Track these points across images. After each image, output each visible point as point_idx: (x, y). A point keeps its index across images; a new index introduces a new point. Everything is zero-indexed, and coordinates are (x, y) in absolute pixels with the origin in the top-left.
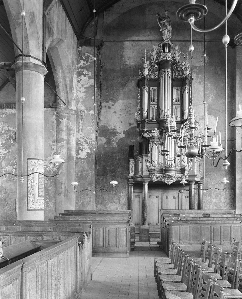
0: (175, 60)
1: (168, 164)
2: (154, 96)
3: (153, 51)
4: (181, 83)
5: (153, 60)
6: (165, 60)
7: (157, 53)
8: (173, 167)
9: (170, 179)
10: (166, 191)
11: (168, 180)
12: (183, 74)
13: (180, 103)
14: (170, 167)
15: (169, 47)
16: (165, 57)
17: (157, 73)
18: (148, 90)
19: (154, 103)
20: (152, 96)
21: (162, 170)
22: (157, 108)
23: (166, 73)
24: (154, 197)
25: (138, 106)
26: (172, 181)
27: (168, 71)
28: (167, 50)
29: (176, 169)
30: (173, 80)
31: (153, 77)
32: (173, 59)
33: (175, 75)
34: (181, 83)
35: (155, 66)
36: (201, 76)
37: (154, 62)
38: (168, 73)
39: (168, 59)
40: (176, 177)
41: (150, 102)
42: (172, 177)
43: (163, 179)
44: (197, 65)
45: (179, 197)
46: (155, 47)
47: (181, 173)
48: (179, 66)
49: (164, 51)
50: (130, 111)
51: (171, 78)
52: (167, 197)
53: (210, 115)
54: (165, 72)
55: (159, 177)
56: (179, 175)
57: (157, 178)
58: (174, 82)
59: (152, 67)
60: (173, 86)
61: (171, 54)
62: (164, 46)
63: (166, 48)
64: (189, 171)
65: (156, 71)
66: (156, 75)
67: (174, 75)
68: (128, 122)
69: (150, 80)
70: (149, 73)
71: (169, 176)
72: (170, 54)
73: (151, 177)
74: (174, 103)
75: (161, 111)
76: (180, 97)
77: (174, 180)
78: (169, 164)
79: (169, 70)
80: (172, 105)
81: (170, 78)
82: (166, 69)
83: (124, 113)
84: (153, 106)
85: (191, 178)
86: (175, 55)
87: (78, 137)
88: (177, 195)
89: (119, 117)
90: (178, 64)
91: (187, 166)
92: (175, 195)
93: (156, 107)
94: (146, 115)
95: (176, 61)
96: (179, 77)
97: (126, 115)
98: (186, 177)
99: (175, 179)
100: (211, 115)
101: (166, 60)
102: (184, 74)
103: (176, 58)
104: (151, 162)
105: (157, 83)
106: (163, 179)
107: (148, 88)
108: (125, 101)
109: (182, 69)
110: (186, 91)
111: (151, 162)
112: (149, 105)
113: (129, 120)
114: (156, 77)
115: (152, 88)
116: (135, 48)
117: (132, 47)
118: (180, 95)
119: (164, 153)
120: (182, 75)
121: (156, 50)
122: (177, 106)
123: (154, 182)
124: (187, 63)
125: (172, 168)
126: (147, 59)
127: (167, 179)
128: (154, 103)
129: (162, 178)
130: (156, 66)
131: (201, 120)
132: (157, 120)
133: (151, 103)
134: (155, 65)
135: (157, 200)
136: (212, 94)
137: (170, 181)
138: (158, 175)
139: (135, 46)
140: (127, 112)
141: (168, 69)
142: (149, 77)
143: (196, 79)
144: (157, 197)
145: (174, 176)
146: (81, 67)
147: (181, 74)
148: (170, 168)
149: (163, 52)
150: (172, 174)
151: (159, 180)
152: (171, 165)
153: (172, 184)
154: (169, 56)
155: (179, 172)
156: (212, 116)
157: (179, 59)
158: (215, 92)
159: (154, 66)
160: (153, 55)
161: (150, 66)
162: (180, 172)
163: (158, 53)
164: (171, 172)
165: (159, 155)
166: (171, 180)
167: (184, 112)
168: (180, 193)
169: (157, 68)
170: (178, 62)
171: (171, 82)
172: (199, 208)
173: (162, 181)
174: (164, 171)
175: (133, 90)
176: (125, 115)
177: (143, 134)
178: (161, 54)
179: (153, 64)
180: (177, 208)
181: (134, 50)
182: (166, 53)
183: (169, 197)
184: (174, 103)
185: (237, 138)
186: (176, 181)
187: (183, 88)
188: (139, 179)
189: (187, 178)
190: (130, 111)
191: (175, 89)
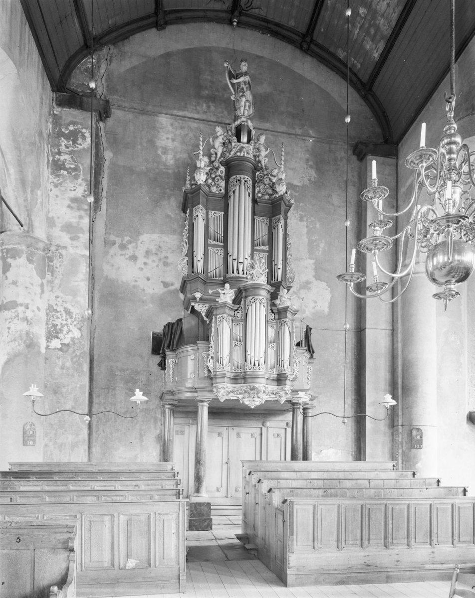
2: (217, 228)
4: (271, 209)
8: (262, 371)
9: (256, 395)
10: (237, 422)
11: (251, 399)
12: (275, 191)
13: (268, 249)
14: (257, 369)
16: (240, 151)
18: (204, 216)
19: (217, 243)
20: (213, 227)
22: (223, 254)
23: (243, 184)
24: (214, 434)
25: (185, 245)
29: (267, 376)
30: (255, 201)
33: (259, 192)
34: (271, 209)
40: (267, 392)
41: (209, 240)
42: (258, 392)
43: (240, 396)
45: (261, 434)
47: (277, 385)
50: (166, 257)
52: (238, 435)
55: (232, 392)
56: (273, 387)
57: (229, 393)
60: (254, 213)
67: (256, 191)
68: (161, 280)
71: (253, 389)
75: (230, 260)
77: (262, 399)
78: (254, 365)
80: (253, 250)
81: (249, 196)
83: (154, 261)
84: (215, 249)
86: (260, 152)
87: (51, 303)
88: (258, 431)
89: (142, 269)
92: (253, 430)
93: (221, 252)
94: (199, 266)
96: (267, 197)
97: (157, 266)
98: (286, 393)
99: (266, 398)
102: (277, 193)
103: (260, 158)
105: (224, 202)
106: (240, 396)
107: (204, 211)
108: (155, 236)
109: (271, 181)
114: (220, 190)
115: (213, 212)
120: (272, 195)
122: (262, 253)
123: (222, 400)
124: (283, 169)
125: (260, 373)
127: (250, 397)
128: (217, 243)
132: (222, 278)
140: (160, 260)
144: (220, 434)
145: (263, 392)
147: (270, 191)
148: (255, 373)
150: (261, 385)
151: (232, 398)
152: (259, 365)
153: (258, 408)
162: (276, 383)
164: (259, 380)
166: (256, 399)
167: (276, 267)
168: (263, 428)
171: (251, 204)
172: (305, 458)
173: (238, 400)
175: (173, 216)
176: (155, 265)
177: (193, 304)
180: (283, 459)
183: (243, 435)
184: (255, 248)
186: (266, 401)
188: (188, 395)
189: (289, 396)
190: (166, 257)
191: (258, 219)
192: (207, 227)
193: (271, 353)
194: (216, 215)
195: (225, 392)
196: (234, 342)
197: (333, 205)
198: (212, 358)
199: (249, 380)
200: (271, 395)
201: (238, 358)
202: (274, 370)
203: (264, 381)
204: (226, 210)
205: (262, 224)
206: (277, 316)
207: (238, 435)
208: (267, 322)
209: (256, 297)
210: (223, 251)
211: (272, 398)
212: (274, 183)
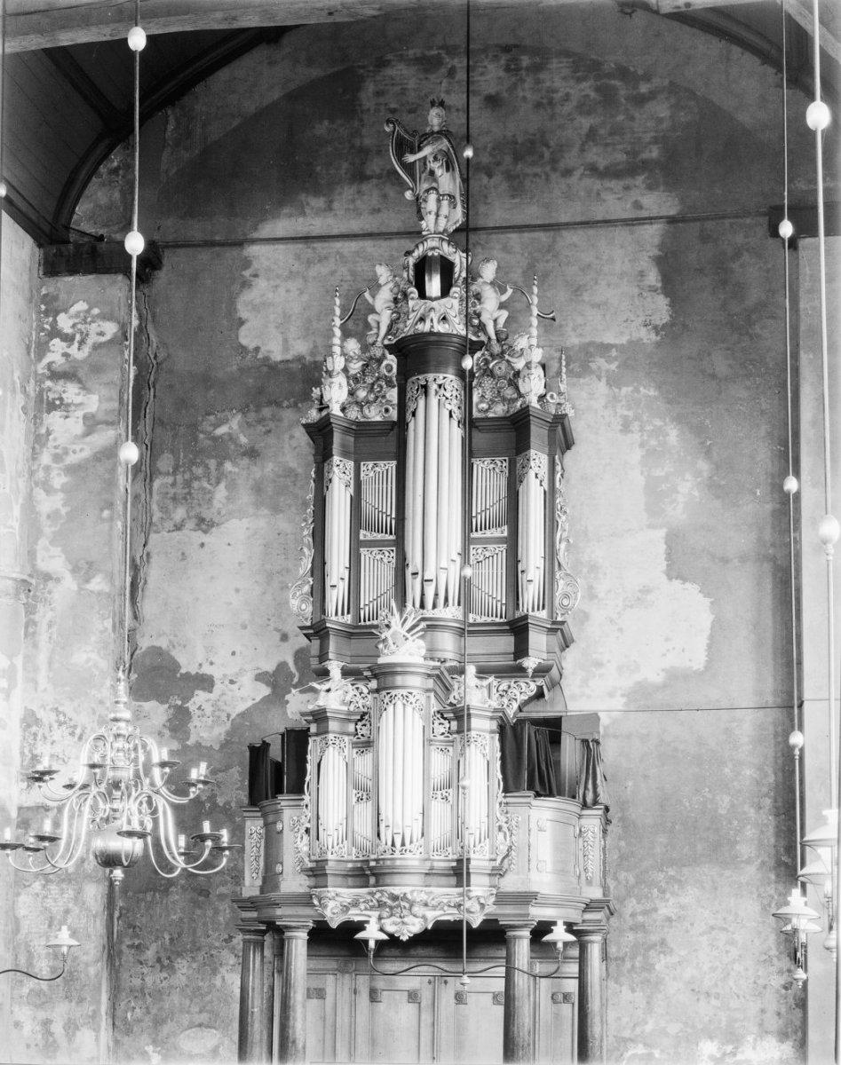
0: (482, 327)
1: (390, 843)
2: (379, 502)
3: (375, 286)
5: (378, 335)
6: (423, 334)
7: (396, 300)
9: (405, 912)
13: (506, 534)
15: (446, 268)
17: (393, 394)
19: (379, 536)
20: (370, 500)
21: (361, 869)
22: (394, 561)
25: (306, 550)
26: (416, 921)
27: (440, 386)
28: (434, 285)
30: (471, 424)
31: (374, 414)
32: (468, 323)
34: (507, 435)
35: (385, 363)
36: (630, 389)
37: (379, 344)
38: (442, 391)
39: (441, 328)
41: (362, 532)
44: (609, 338)
46: (383, 273)
48: (501, 355)
49: (422, 295)
51: (457, 414)
53: (677, 583)
54: (425, 388)
55: (355, 904)
57: (346, 909)
58: (476, 434)
59: (370, 363)
60: (470, 453)
61: (456, 303)
62: (422, 268)
63: (430, 280)
64: (497, 873)
65: (390, 384)
66: (389, 402)
67: (475, 398)
69: (361, 430)
70: (351, 393)
72: (453, 305)
73: (316, 902)
74: (474, 535)
75: (409, 572)
76: (504, 502)
77: (424, 917)
78: (393, 845)
79: (450, 380)
80: (467, 541)
81: (451, 416)
82: (431, 376)
84: (375, 550)
85: (509, 910)
90: (496, 349)
91: (487, 848)
93: (390, 556)
95: (486, 333)
99: (432, 916)
100: (684, 580)
101: (431, 333)
104: (313, 832)
105: (389, 440)
107: (350, 464)
109: (513, 368)
110: (532, 474)
111: (313, 832)
112: (356, 545)
113: (279, 616)
114: (387, 410)
115: (371, 464)
116: (313, 272)
117: (297, 267)
118: (504, 493)
119: (368, 791)
120: (515, 400)
121: (391, 285)
122: (491, 547)
123: (334, 925)
126: (342, 327)
128: (379, 536)
129: (366, 909)
130: (391, 360)
131: (631, 607)
133: (364, 535)
134: (384, 357)
135: (411, 1009)
136: (688, 476)
137: (403, 923)
138: (348, 894)
139: (309, 263)
141: (441, 376)
142: (353, 414)
143: (606, 407)
146: (55, 375)
147: (509, 393)
148: (388, 863)
149: (416, 295)
152: (403, 844)
154: (442, 314)
155: (443, 880)
156: (688, 585)
157: (501, 322)
158: (704, 466)
159: (380, 361)
160: (378, 308)
161: (361, 363)
162: (453, 880)
163: (400, 299)
164: (397, 879)
165: (355, 799)
169: (395, 370)
170: (493, 337)
174: (374, 874)
175: (300, 470)
178: (411, 303)
179: (378, 352)
181: (288, 290)
182: (432, 299)
185: (807, 695)
186: (438, 924)
187: (520, 460)
189: (488, 910)
192: (356, 502)
193: (440, 811)
194: (377, 469)
195: (338, 904)
196: (355, 792)
197: (713, 376)
198: (307, 831)
199: (388, 880)
200: (446, 908)
201: (364, 828)
202: (450, 849)
203: (416, 879)
204: (401, 457)
205: (490, 475)
206: (454, 725)
207: (374, 996)
208: (428, 742)
209: (393, 692)
210: (393, 554)
211: (450, 915)
212: (517, 374)
